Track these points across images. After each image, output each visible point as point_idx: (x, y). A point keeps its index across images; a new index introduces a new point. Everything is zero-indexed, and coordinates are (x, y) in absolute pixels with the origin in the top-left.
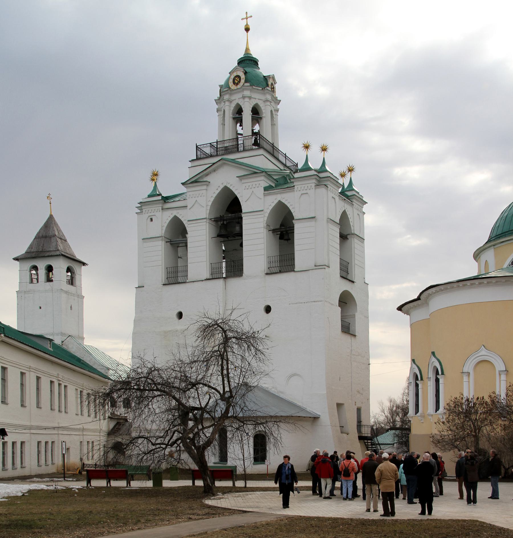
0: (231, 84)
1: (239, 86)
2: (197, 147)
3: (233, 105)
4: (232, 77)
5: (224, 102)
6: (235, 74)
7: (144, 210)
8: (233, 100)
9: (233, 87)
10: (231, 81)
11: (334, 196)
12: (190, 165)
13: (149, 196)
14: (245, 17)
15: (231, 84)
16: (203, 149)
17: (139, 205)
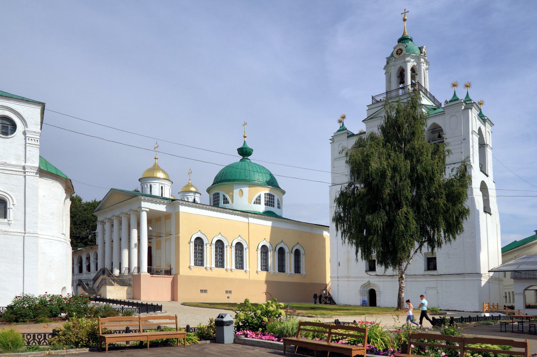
0: (395, 55)
1: (400, 56)
2: (372, 97)
3: (398, 67)
4: (396, 50)
5: (391, 67)
6: (398, 48)
7: (335, 141)
8: (396, 65)
9: (396, 56)
10: (395, 52)
11: (475, 116)
12: (367, 108)
13: (339, 131)
14: (403, 12)
15: (395, 55)
16: (375, 98)
17: (332, 138)
